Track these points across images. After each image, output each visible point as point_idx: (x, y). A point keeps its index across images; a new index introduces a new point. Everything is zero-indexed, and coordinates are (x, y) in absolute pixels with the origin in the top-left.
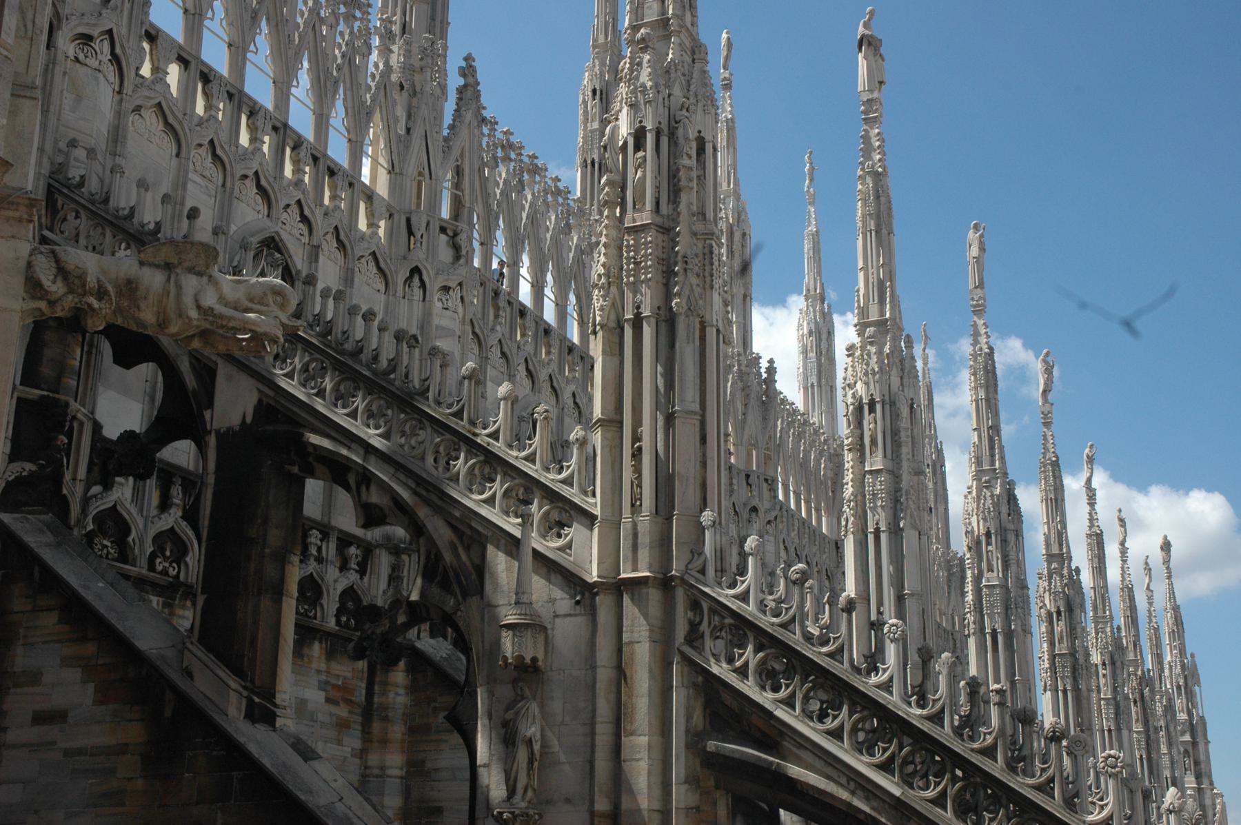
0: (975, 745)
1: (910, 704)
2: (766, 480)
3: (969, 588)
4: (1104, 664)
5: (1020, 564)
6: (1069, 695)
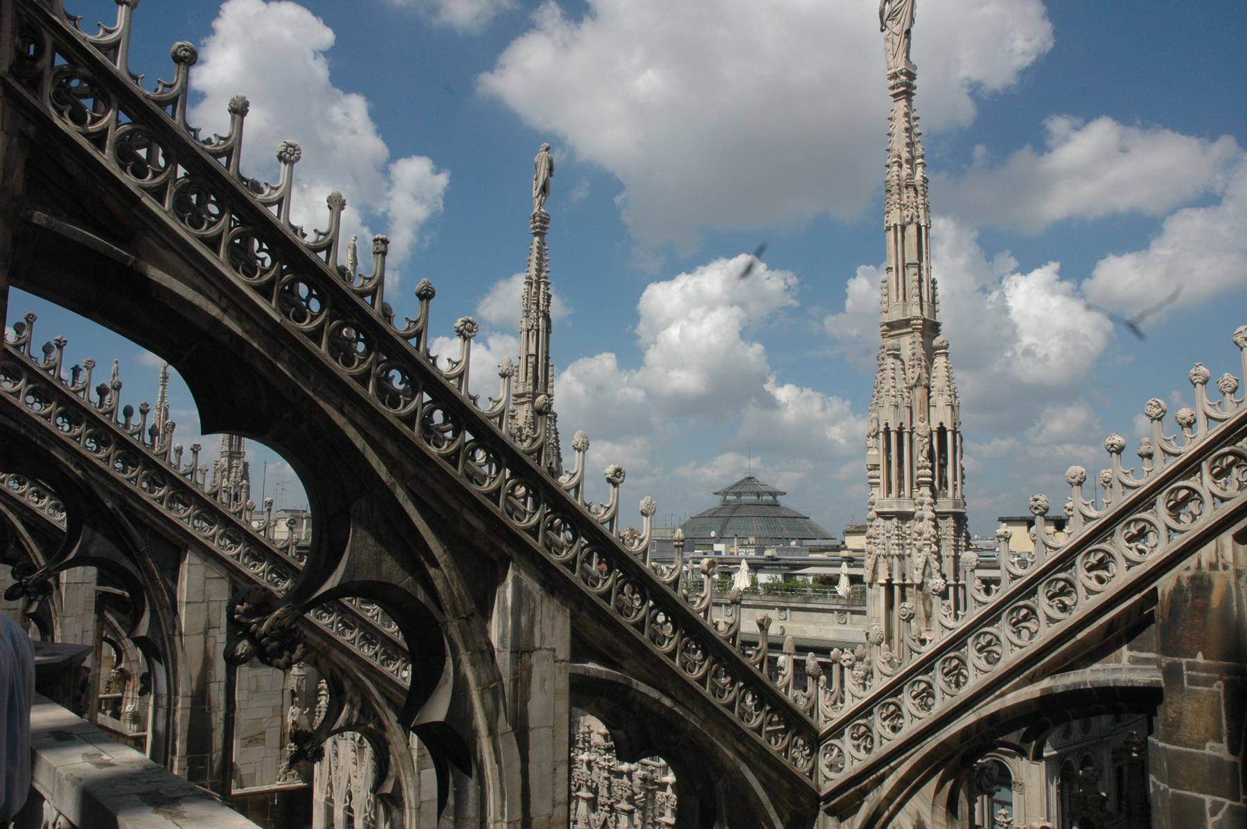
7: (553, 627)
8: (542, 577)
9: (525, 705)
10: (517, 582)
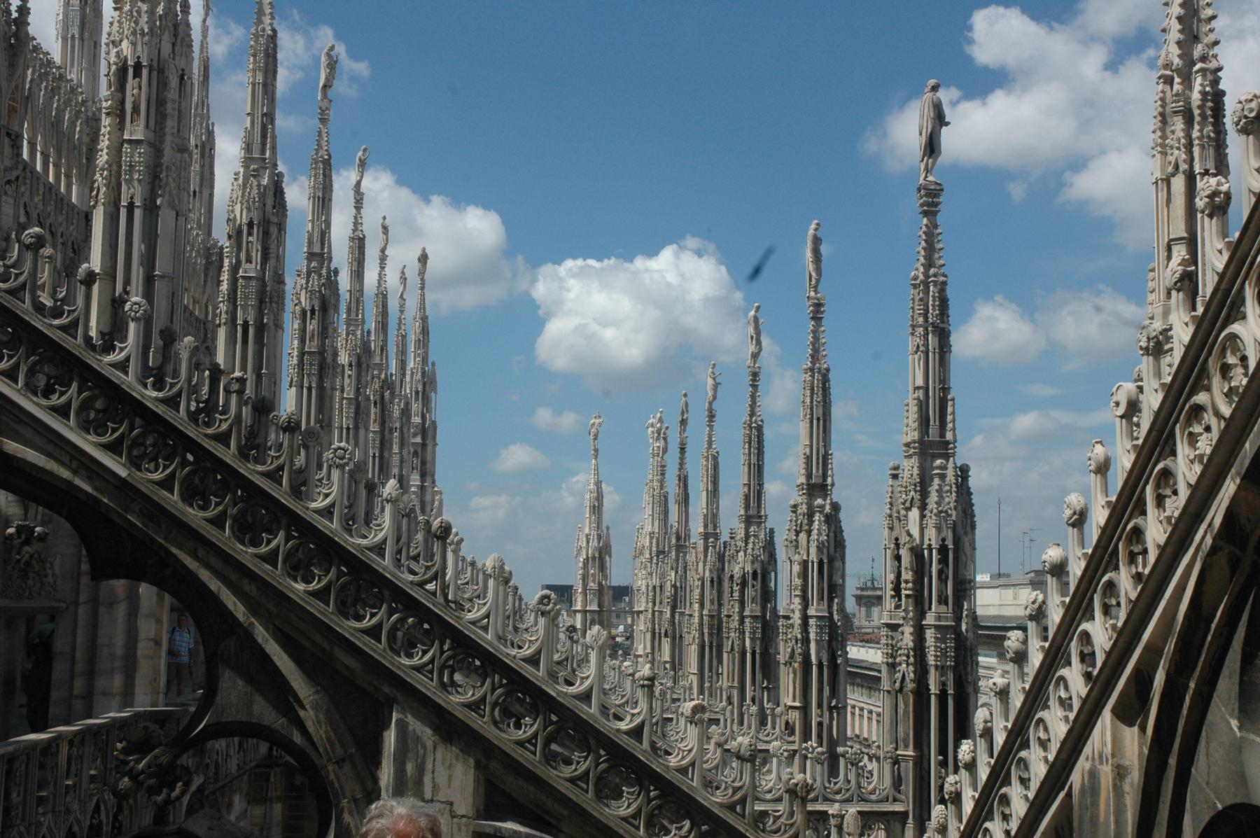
0: (210, 431)
1: (145, 386)
2: (9, 135)
3: (225, 277)
4: (350, 365)
5: (280, 259)
6: (314, 392)
7: (450, 777)
10: (402, 726)
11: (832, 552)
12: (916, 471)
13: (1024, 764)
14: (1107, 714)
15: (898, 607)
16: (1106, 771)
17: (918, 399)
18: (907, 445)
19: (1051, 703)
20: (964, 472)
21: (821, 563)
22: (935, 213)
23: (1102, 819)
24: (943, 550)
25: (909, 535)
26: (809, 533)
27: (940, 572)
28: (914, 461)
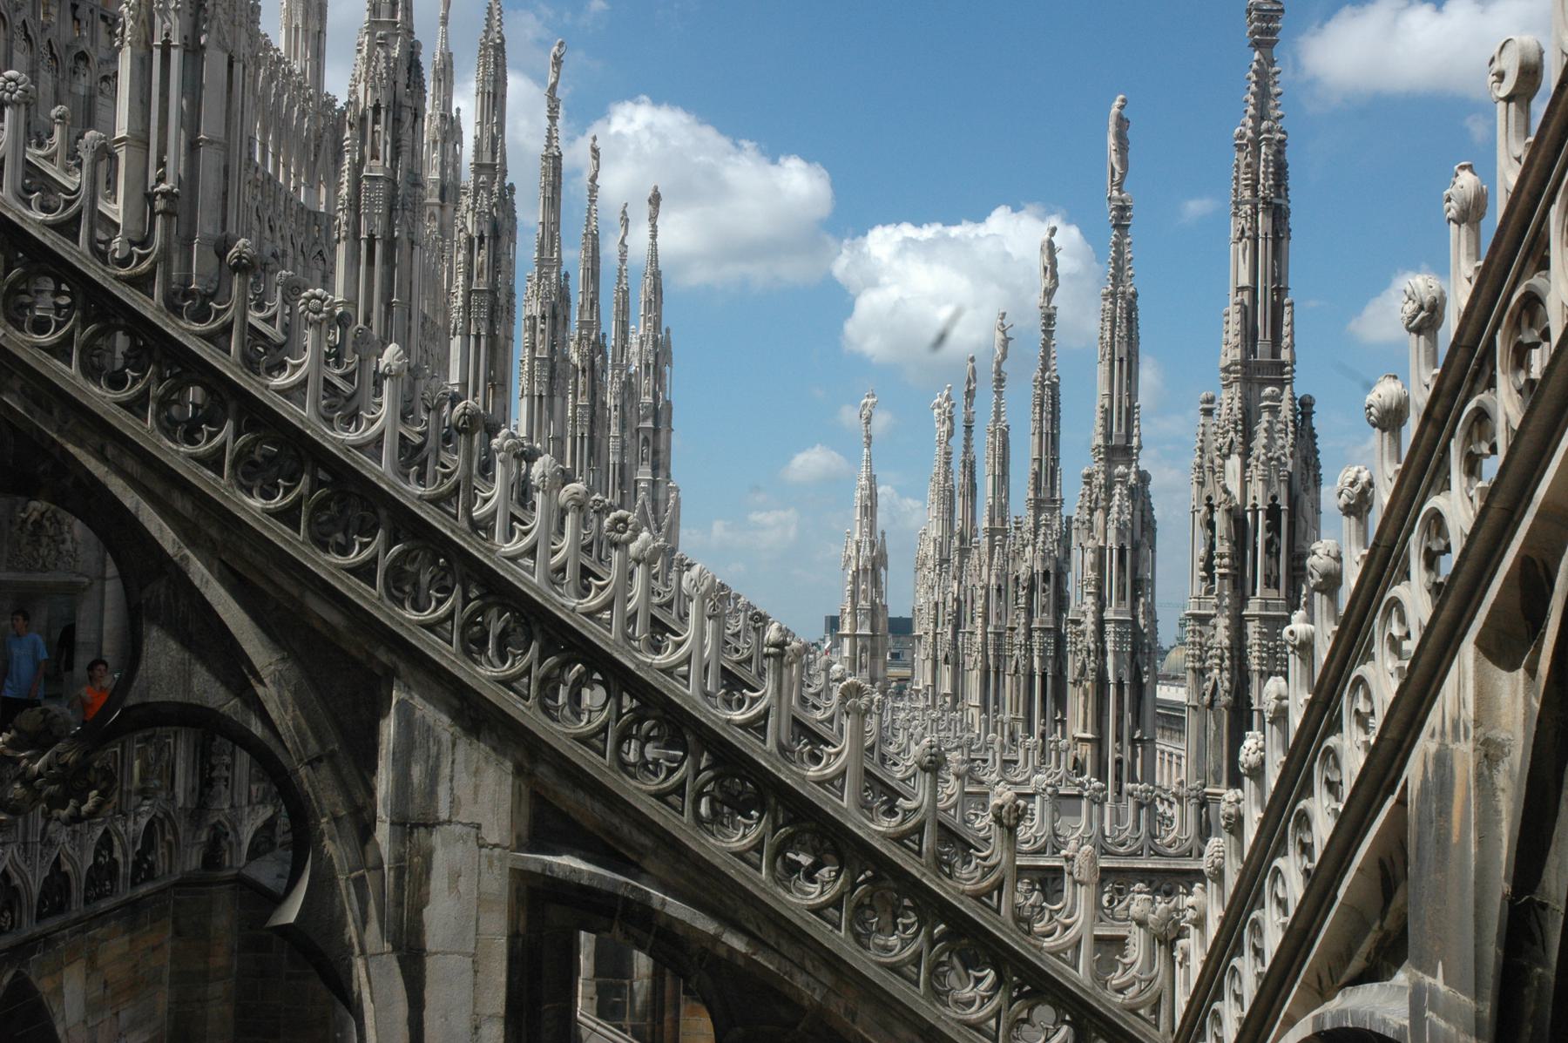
0: (123, 272)
1: (28, 204)
2: (104, 18)
3: (345, 177)
4: (543, 317)
5: (415, 153)
6: (483, 341)
7: (476, 787)
8: (455, 702)
9: (419, 912)
10: (406, 711)
11: (1137, 535)
12: (1237, 404)
13: (1332, 757)
14: (1468, 650)
15: (1209, 592)
16: (1465, 754)
17: (1241, 303)
18: (1226, 370)
19: (1376, 649)
20: (1305, 408)
21: (1122, 551)
22: (1272, 44)
23: (1455, 839)
24: (1273, 512)
25: (1226, 491)
26: (1107, 511)
27: (1269, 544)
28: (1236, 390)
